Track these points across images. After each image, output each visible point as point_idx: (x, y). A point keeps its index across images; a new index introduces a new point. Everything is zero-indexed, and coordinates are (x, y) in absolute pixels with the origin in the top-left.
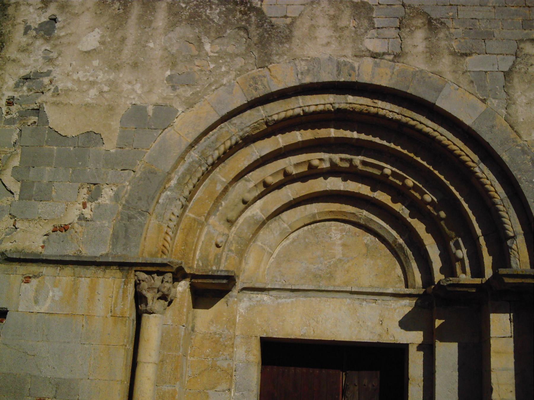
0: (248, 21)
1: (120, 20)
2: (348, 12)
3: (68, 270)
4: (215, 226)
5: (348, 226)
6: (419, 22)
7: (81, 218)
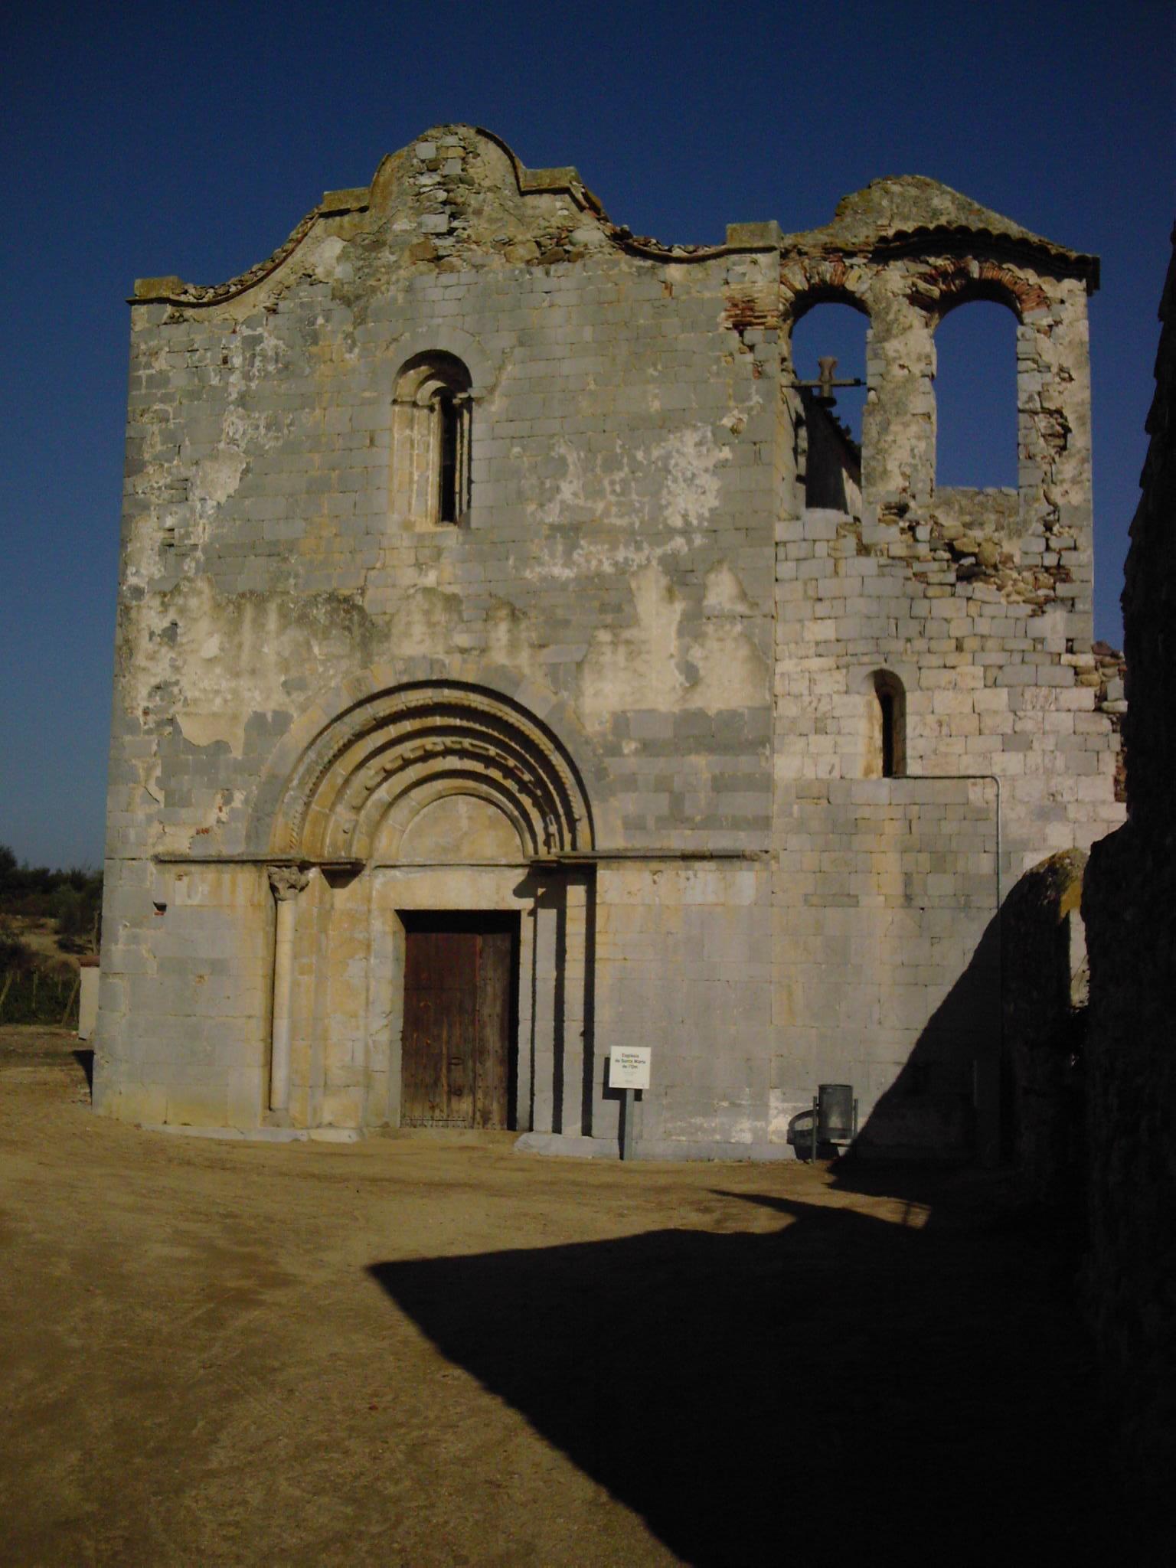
0: (351, 620)
1: (235, 625)
2: (440, 605)
3: (213, 867)
4: (343, 814)
5: (474, 799)
6: (504, 613)
7: (219, 821)
